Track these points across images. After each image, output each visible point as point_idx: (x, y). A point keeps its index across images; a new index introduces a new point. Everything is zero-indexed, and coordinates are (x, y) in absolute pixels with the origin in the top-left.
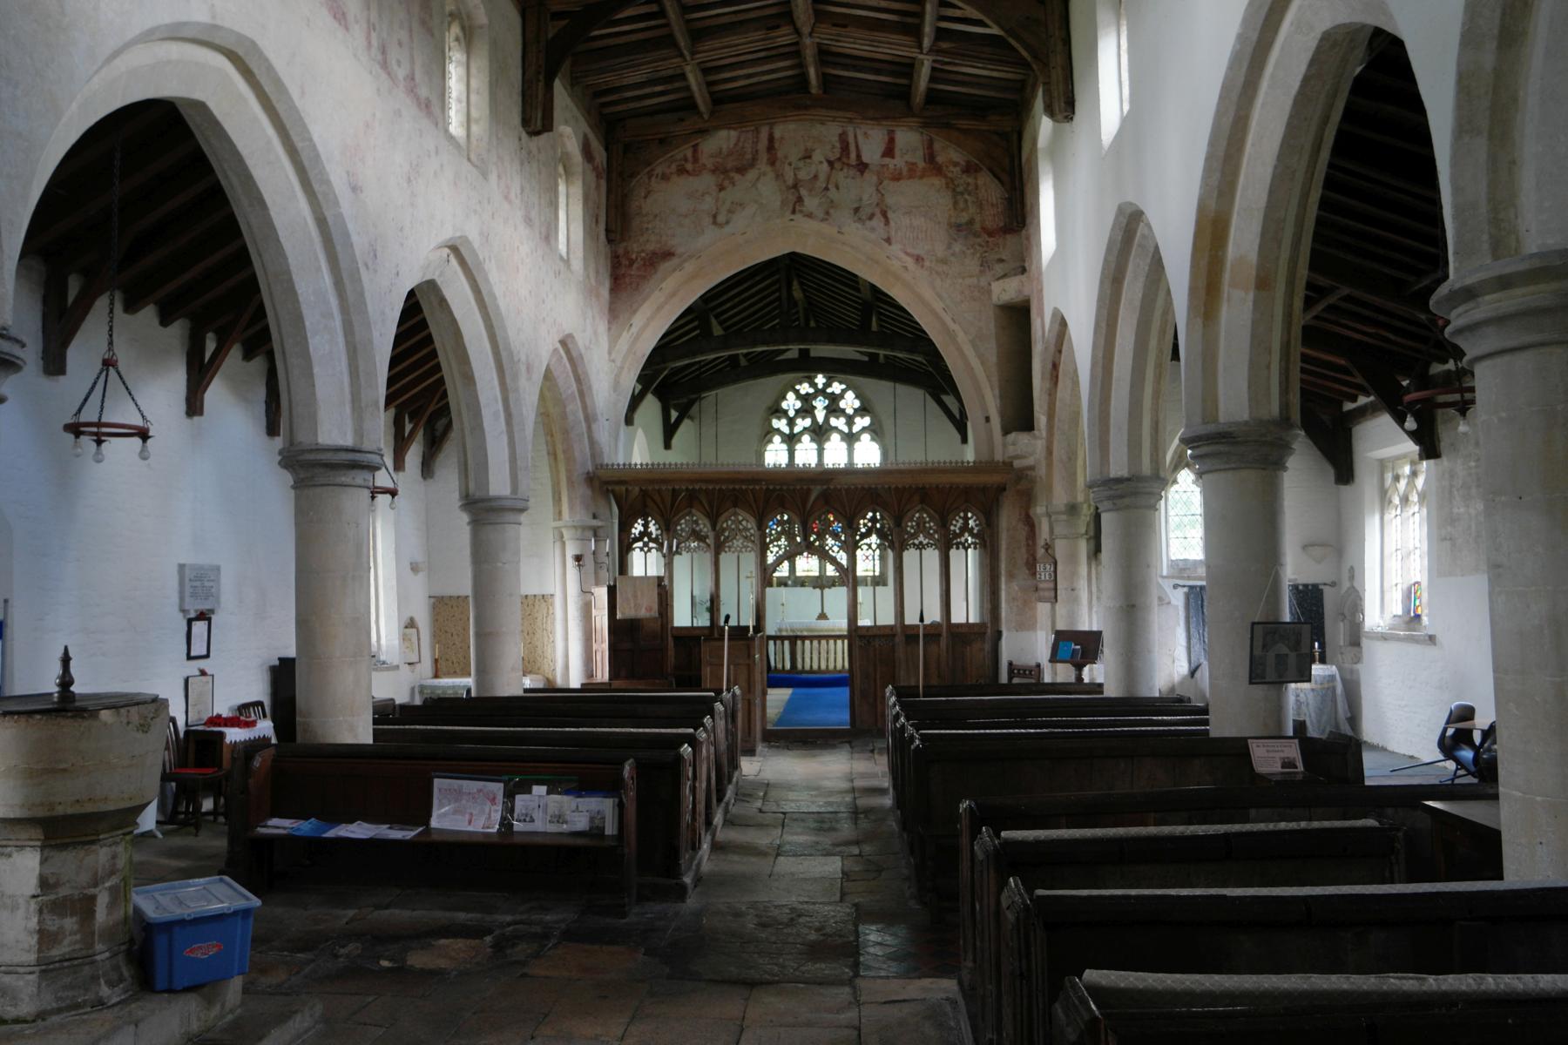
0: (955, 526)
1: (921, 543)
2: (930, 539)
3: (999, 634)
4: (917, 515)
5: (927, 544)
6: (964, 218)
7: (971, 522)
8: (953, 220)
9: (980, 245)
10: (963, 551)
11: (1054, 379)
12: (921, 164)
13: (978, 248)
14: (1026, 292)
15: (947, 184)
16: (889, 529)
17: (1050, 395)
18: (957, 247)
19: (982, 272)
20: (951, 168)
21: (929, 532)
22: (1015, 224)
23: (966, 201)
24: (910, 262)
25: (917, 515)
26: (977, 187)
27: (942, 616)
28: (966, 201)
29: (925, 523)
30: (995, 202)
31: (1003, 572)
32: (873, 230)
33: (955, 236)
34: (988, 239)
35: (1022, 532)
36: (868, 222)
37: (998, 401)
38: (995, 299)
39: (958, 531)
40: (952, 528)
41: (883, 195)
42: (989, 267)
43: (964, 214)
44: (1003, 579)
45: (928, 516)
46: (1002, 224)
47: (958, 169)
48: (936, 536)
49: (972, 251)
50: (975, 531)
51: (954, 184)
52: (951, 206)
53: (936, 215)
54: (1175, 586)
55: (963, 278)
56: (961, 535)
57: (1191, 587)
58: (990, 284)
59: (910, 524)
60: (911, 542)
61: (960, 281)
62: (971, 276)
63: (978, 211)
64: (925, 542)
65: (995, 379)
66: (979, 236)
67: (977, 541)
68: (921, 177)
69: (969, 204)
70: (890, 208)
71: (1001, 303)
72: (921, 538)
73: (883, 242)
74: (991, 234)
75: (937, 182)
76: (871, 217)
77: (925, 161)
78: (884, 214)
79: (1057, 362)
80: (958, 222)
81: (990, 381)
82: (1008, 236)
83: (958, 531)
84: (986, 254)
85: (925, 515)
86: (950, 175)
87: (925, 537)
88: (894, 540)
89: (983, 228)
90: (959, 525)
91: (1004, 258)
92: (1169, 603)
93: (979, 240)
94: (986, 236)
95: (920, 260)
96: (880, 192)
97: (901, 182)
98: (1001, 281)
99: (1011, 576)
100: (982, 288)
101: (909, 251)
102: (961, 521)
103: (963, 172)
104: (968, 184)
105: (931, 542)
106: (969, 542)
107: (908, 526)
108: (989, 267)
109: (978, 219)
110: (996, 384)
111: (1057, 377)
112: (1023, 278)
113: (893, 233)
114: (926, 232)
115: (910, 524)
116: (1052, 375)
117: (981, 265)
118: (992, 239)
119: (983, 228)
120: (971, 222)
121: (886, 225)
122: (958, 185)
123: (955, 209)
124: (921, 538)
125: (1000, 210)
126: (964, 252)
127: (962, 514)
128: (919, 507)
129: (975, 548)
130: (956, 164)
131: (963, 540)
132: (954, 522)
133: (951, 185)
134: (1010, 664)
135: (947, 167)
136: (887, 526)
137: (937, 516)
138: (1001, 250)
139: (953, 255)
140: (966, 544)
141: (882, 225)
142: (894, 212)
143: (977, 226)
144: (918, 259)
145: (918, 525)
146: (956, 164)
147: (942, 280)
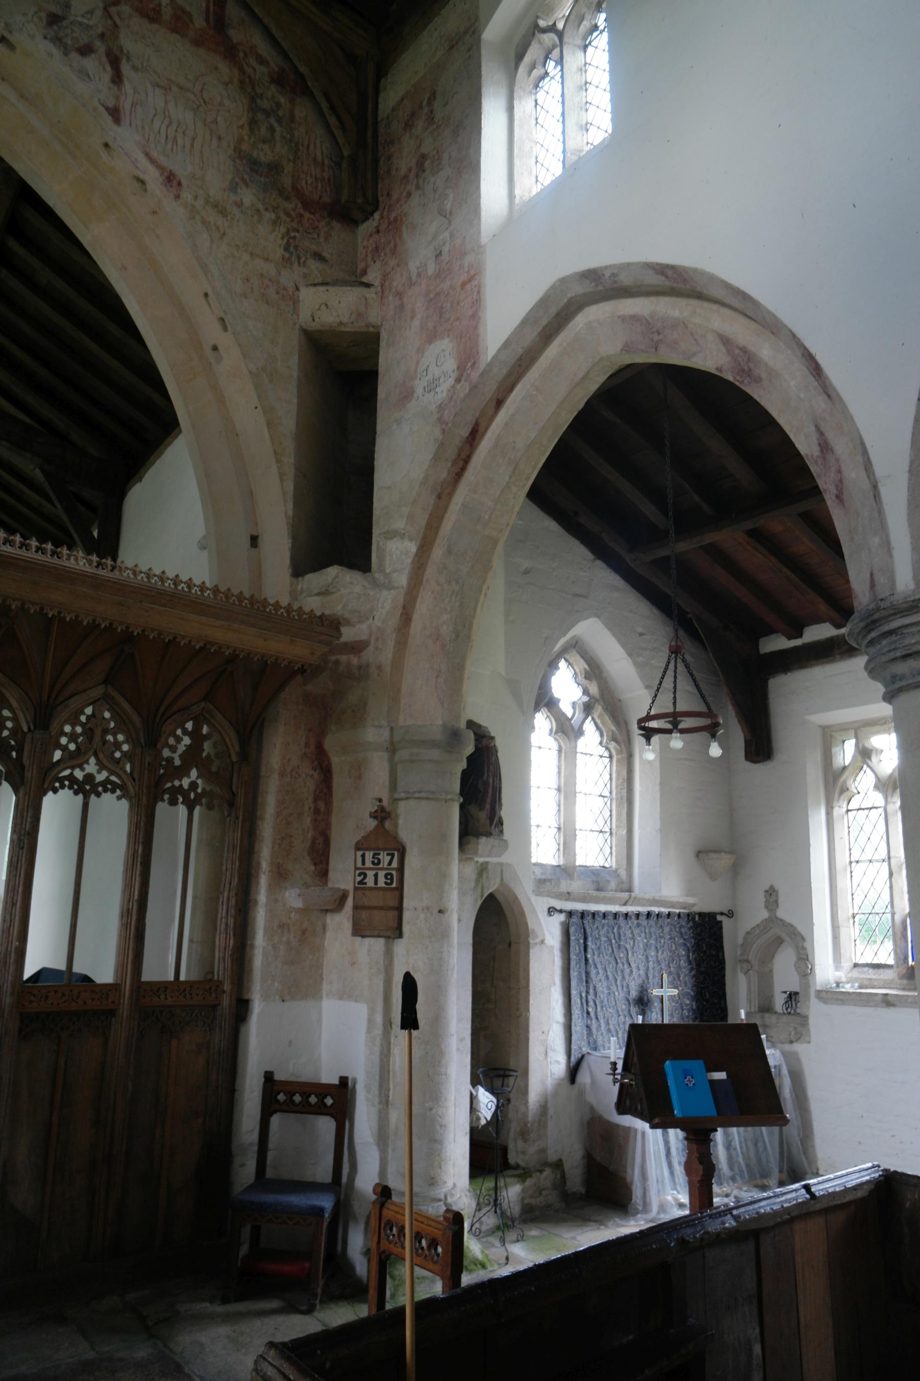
0: (173, 749)
1: (89, 778)
2: (112, 772)
3: (242, 1008)
4: (89, 711)
5: (104, 784)
6: (265, 155)
7: (207, 746)
8: (245, 147)
9: (288, 214)
10: (182, 810)
11: (461, 463)
12: (199, 22)
13: (283, 217)
14: (373, 316)
15: (242, 82)
16: (14, 732)
17: (439, 497)
18: (248, 197)
19: (286, 262)
20: (252, 61)
21: (113, 758)
22: (360, 201)
23: (272, 129)
24: (152, 176)
25: (89, 711)
26: (292, 118)
27: (121, 967)
28: (272, 129)
29: (106, 731)
30: (319, 158)
31: (264, 865)
32: (84, 74)
33: (247, 177)
34: (302, 211)
35: (307, 785)
36: (74, 55)
37: (290, 506)
38: (303, 317)
39: (177, 762)
40: (166, 753)
41: (115, 25)
42: (299, 258)
43: (266, 147)
44: (263, 881)
45: (115, 715)
46: (327, 199)
47: (261, 69)
48: (128, 768)
49: (273, 216)
50: (214, 769)
51: (253, 88)
52: (244, 120)
53: (215, 121)
54: (551, 911)
55: (252, 254)
56: (183, 771)
57: (570, 914)
58: (297, 289)
59: (67, 729)
60: (67, 772)
61: (246, 257)
62: (267, 260)
63: (291, 157)
64: (101, 777)
65: (289, 460)
66: (287, 199)
67: (217, 790)
68: (197, 43)
69: (277, 135)
70: (128, 59)
71: (314, 326)
72: (91, 767)
73: (102, 109)
74: (307, 205)
75: (224, 68)
76: (86, 50)
77: (207, 20)
78: (115, 61)
79: (481, 429)
80: (255, 155)
81: (278, 461)
82: (336, 225)
83: (177, 762)
84: (297, 235)
85: (107, 715)
86: (249, 71)
87: (101, 767)
88: (26, 761)
89: (295, 188)
90: (181, 748)
91: (325, 254)
92: (543, 942)
93: (286, 205)
94: (300, 206)
95: (175, 183)
96: (111, 17)
97: (155, 26)
98: (322, 289)
99: (281, 875)
100: (284, 289)
101: (154, 154)
102: (187, 740)
103: (273, 81)
104: (278, 105)
105: (113, 778)
106: (199, 790)
107: (63, 733)
108: (299, 258)
109: (289, 168)
110: (290, 471)
111: (467, 461)
112: (370, 294)
113: (126, 105)
114: (193, 139)
115: (67, 729)
116: (461, 450)
117: (286, 249)
118: (307, 215)
119: (295, 188)
120: (274, 168)
121: (113, 81)
122: (261, 96)
123: (251, 130)
124: (91, 767)
125: (326, 175)
126: (258, 211)
127: (189, 725)
128: (99, 691)
129: (210, 807)
130: (262, 61)
131: (186, 783)
132: (171, 741)
133: (249, 90)
134: (269, 1077)
135: (246, 55)
136: (9, 724)
137: (136, 719)
138: (322, 240)
139: (239, 205)
140: (192, 796)
141: (107, 77)
142: (135, 68)
143: (287, 181)
144: (170, 179)
145: (89, 732)
146: (262, 61)
147: (212, 241)
